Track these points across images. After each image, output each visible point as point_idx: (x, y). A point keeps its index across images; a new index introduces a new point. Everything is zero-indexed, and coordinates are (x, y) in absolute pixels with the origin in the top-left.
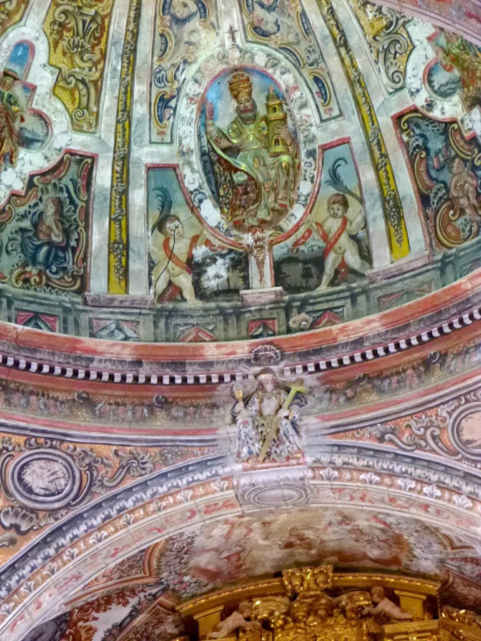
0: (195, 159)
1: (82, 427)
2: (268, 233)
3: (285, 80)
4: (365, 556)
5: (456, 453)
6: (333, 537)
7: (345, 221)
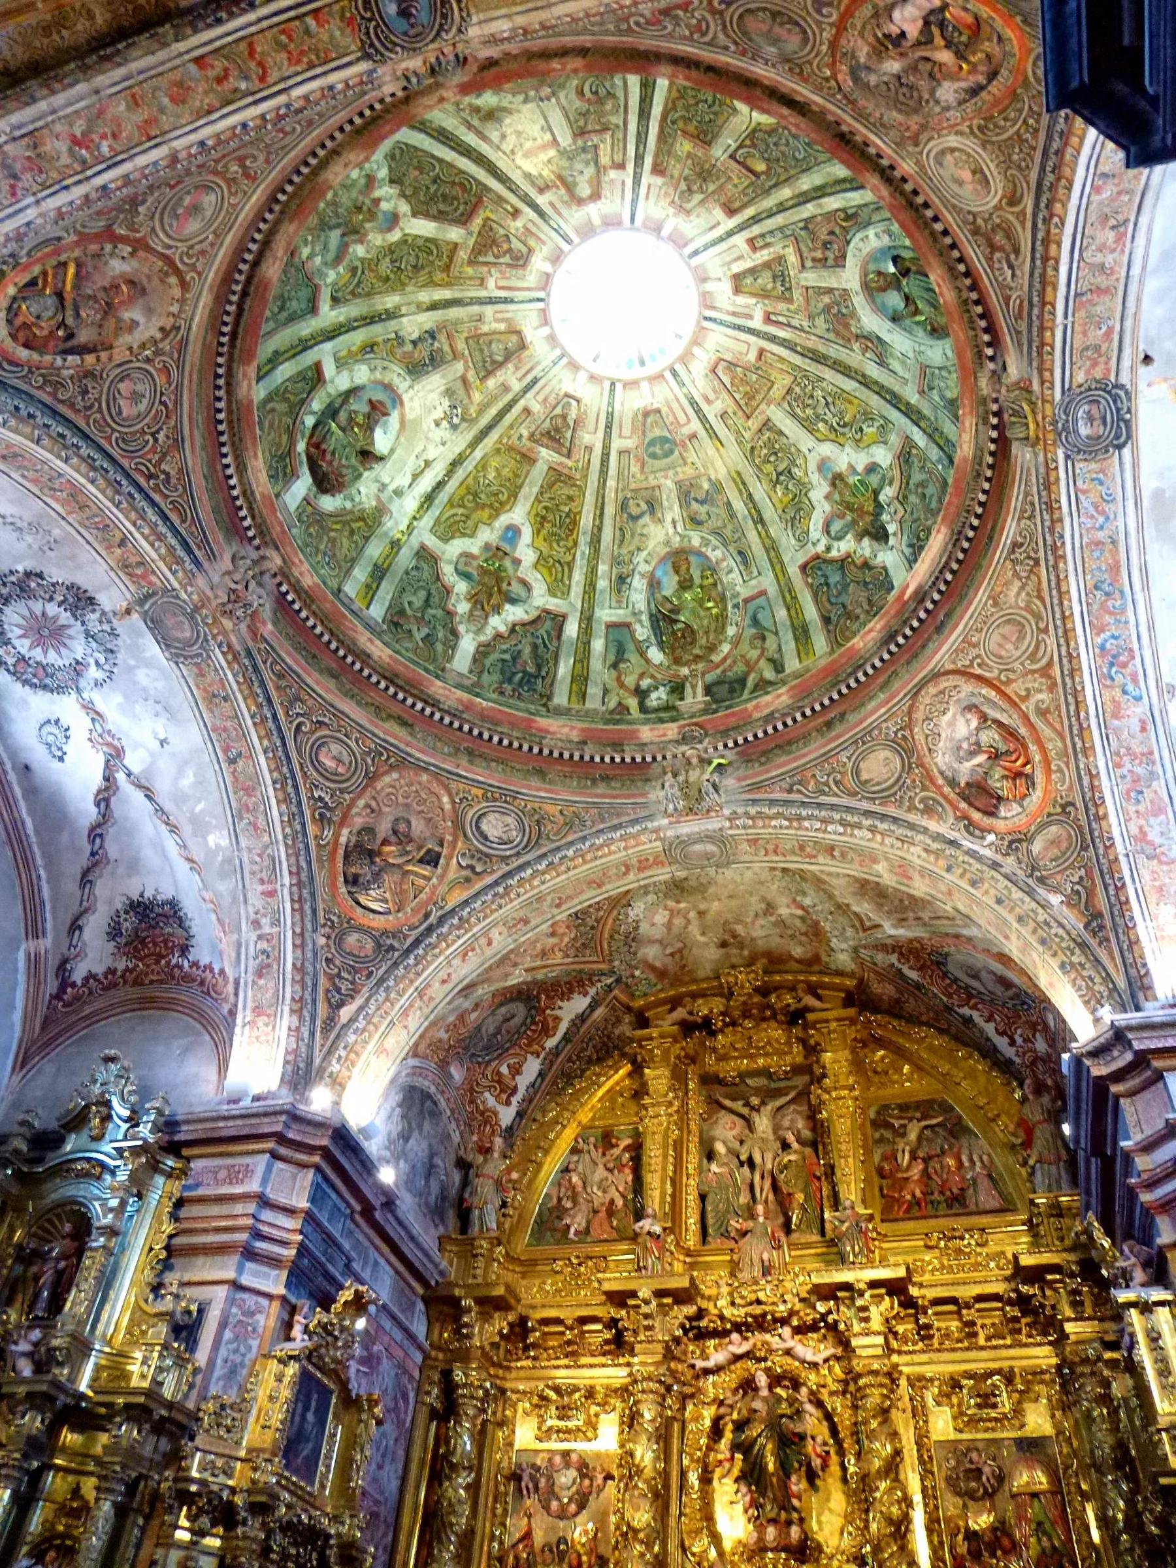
0: (645, 618)
1: (534, 791)
2: (701, 666)
3: (714, 555)
4: (791, 957)
5: (855, 794)
6: (760, 932)
7: (763, 650)
